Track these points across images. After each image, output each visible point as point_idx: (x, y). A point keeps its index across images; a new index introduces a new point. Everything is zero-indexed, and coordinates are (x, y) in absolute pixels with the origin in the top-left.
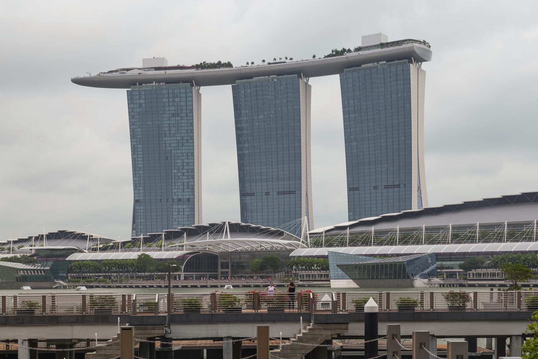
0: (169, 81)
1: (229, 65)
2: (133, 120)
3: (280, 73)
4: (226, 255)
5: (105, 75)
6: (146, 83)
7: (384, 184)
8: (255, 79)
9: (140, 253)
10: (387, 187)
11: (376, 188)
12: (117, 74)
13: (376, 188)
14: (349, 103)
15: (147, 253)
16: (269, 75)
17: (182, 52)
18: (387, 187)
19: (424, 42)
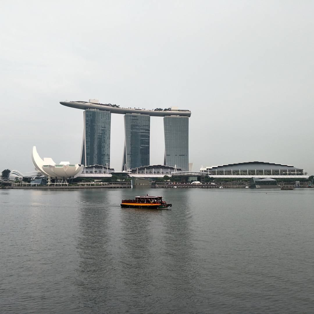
0: (101, 109)
1: (117, 107)
2: (87, 122)
3: (142, 113)
4: (176, 177)
5: (76, 103)
6: (92, 109)
7: (179, 154)
8: (133, 114)
9: (164, 175)
10: (180, 155)
11: (176, 155)
12: (80, 103)
13: (176, 155)
14: (167, 127)
15: (167, 175)
16: (138, 113)
17: (102, 98)
18: (180, 155)
19: (190, 111)
